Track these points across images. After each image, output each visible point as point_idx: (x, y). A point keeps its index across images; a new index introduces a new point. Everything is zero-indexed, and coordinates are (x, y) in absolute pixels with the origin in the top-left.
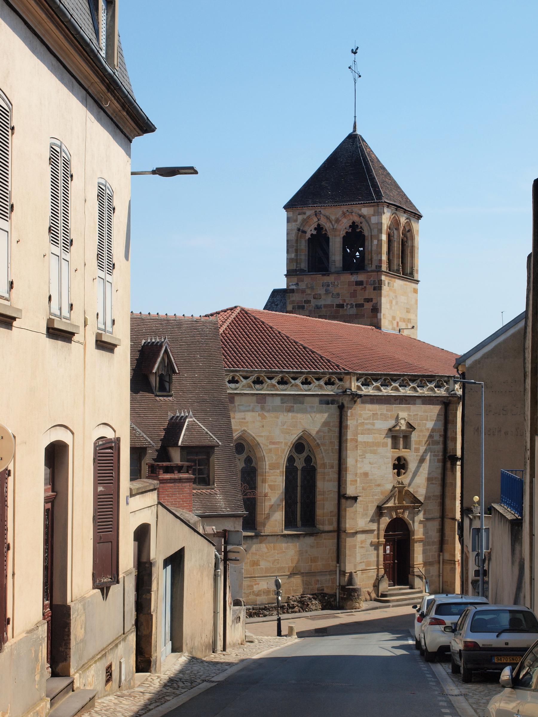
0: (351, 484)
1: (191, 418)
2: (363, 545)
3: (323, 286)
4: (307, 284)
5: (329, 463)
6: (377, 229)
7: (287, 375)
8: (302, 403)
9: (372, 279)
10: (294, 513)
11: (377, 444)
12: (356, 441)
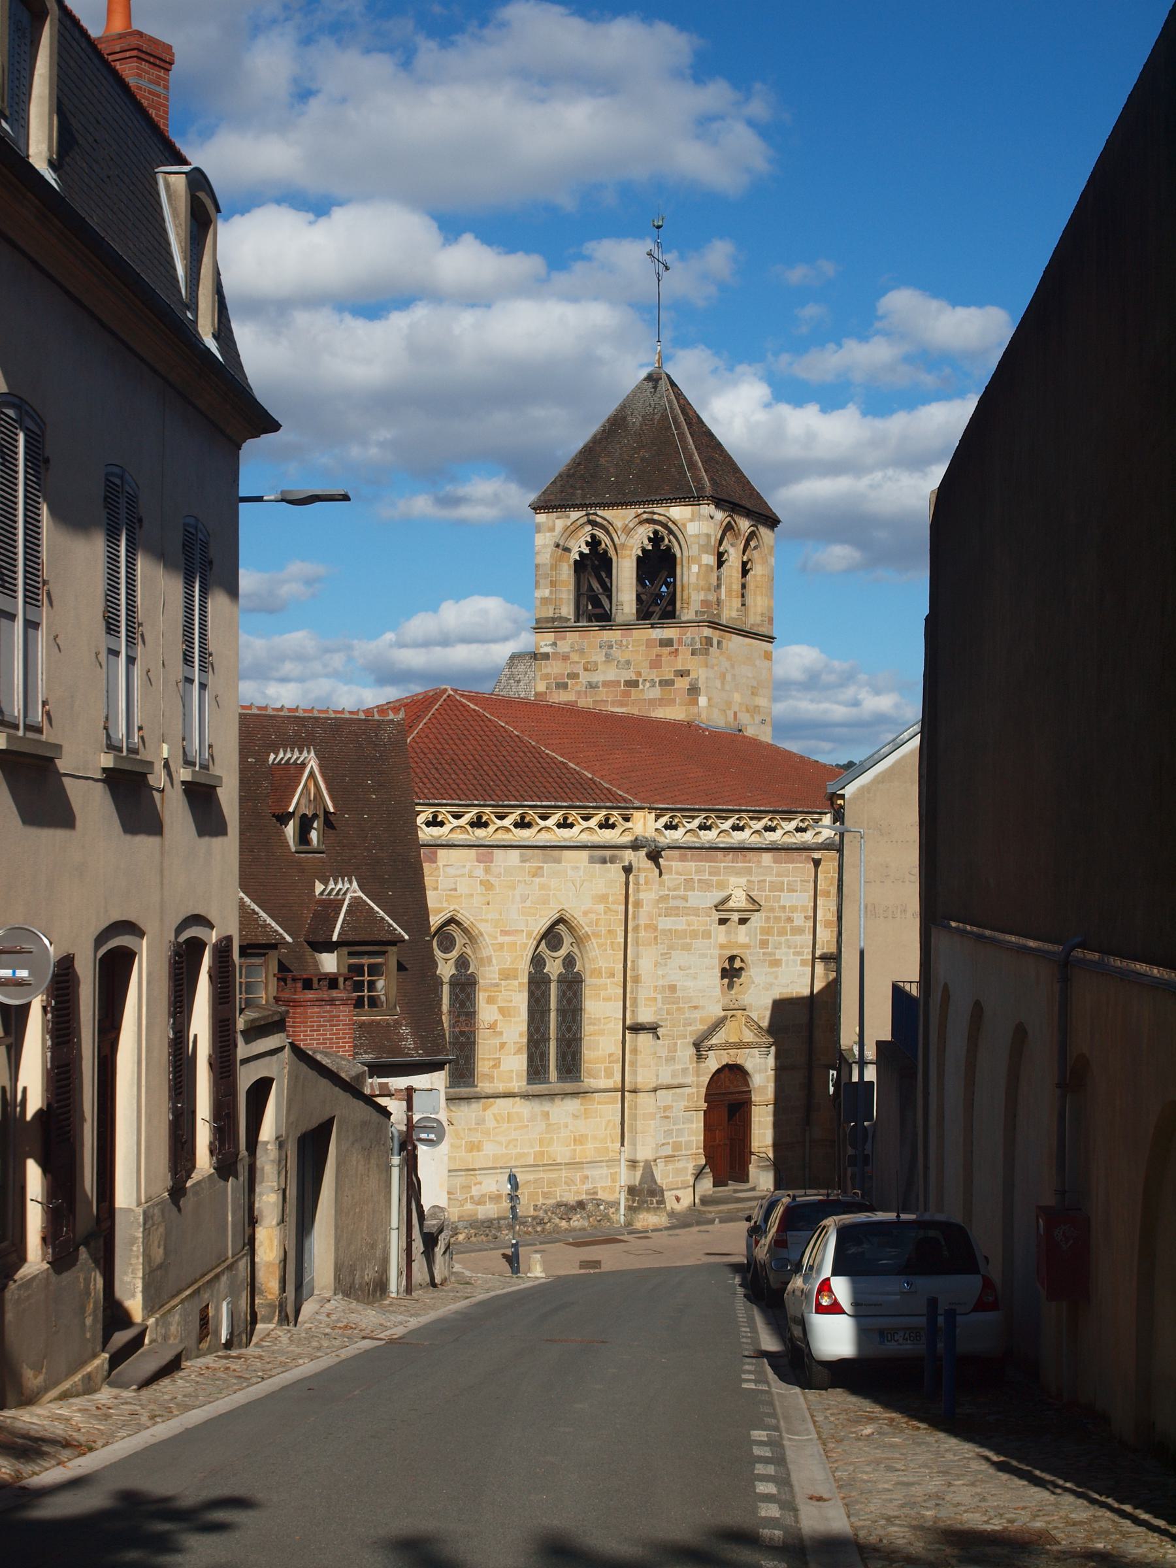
0: (646, 1005)
1: (355, 892)
3: (600, 647)
4: (572, 643)
5: (606, 968)
6: (697, 546)
7: (530, 812)
8: (559, 861)
9: (688, 635)
10: (544, 1056)
11: (694, 935)
12: (656, 929)
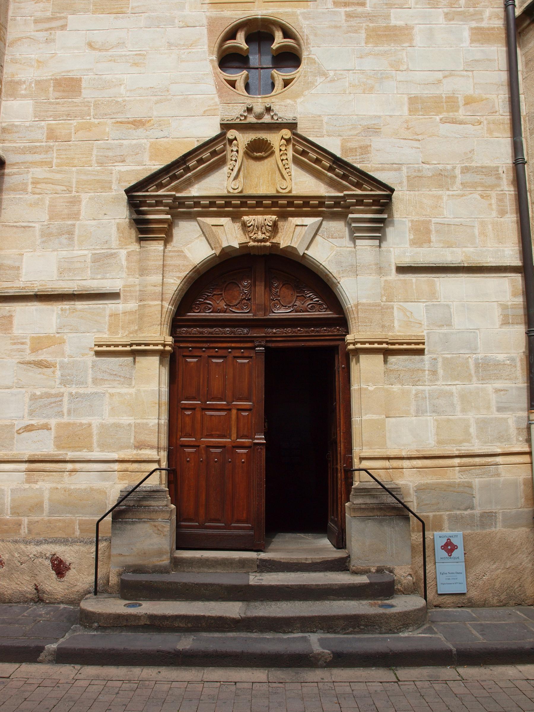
2: (43, 356)
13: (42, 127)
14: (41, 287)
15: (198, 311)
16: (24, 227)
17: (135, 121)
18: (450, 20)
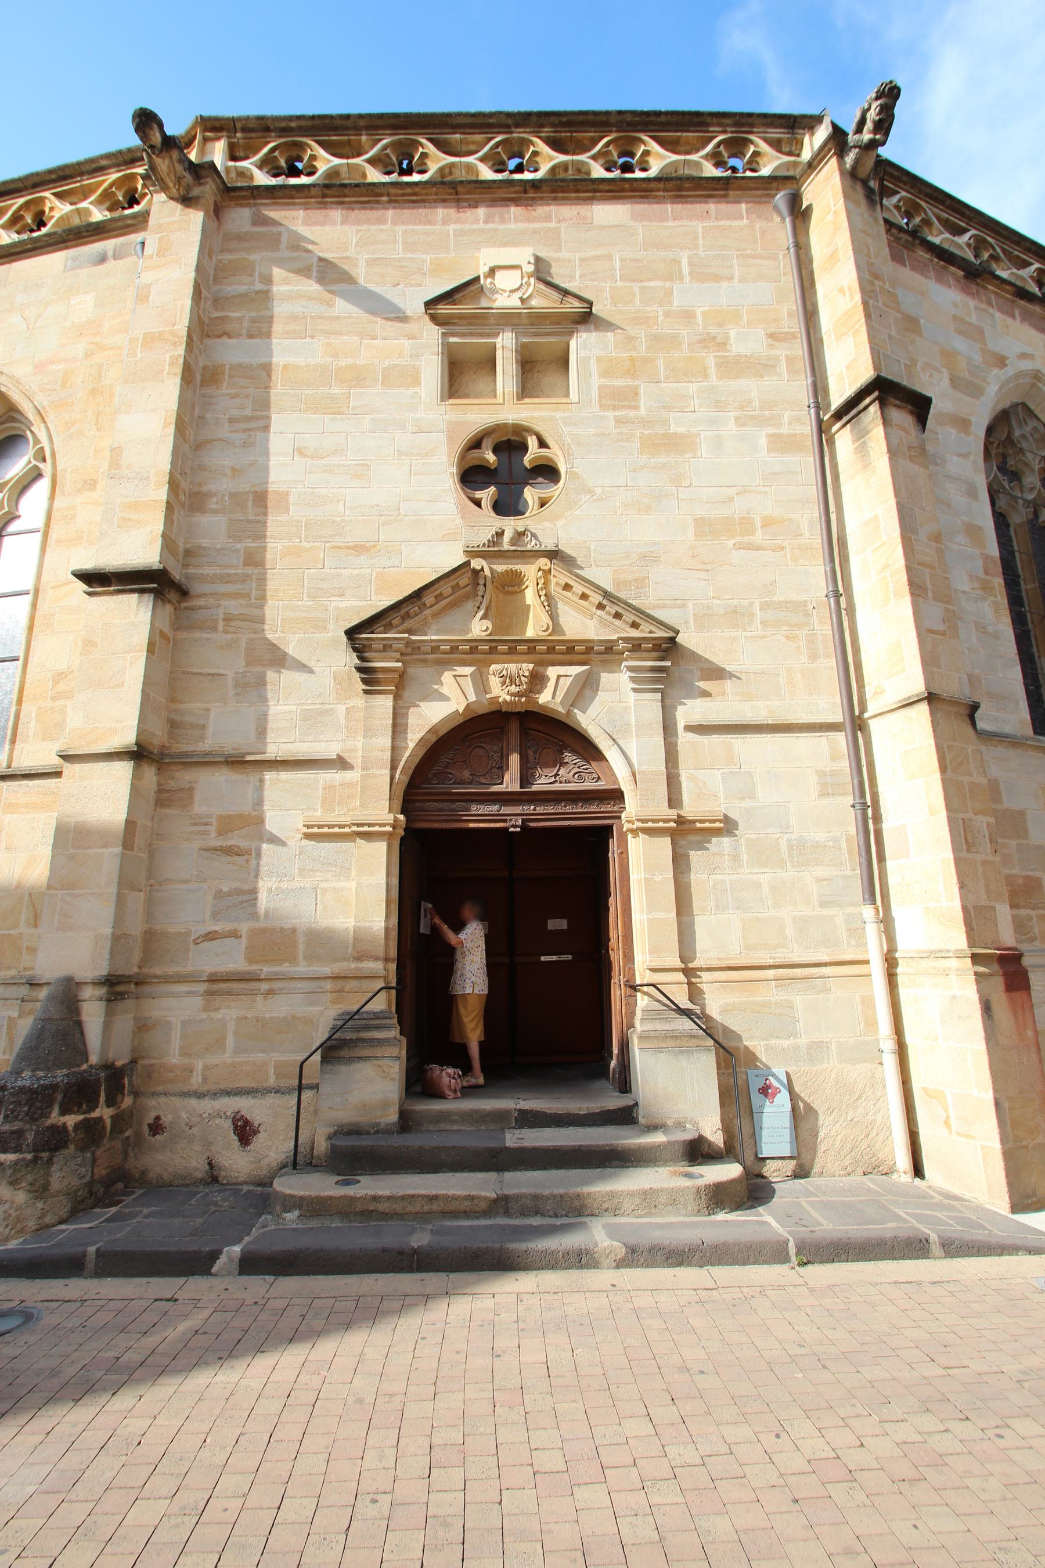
13: (238, 551)
14: (233, 752)
15: (436, 782)
16: (212, 675)
17: (356, 546)
18: (742, 426)
